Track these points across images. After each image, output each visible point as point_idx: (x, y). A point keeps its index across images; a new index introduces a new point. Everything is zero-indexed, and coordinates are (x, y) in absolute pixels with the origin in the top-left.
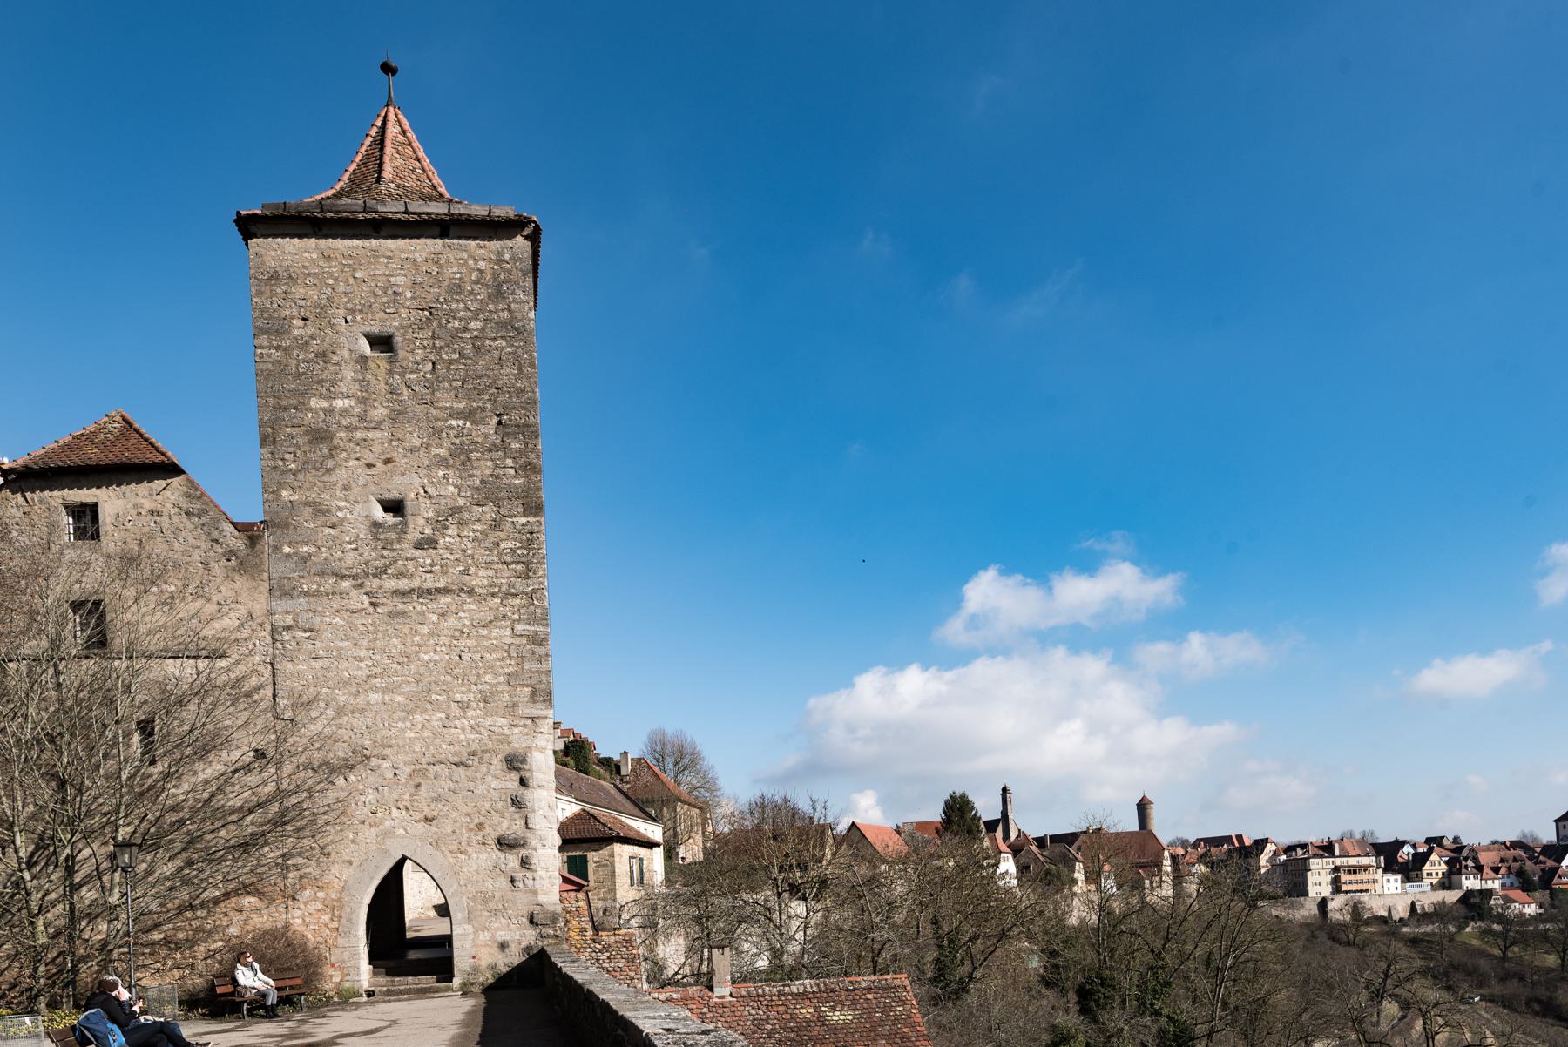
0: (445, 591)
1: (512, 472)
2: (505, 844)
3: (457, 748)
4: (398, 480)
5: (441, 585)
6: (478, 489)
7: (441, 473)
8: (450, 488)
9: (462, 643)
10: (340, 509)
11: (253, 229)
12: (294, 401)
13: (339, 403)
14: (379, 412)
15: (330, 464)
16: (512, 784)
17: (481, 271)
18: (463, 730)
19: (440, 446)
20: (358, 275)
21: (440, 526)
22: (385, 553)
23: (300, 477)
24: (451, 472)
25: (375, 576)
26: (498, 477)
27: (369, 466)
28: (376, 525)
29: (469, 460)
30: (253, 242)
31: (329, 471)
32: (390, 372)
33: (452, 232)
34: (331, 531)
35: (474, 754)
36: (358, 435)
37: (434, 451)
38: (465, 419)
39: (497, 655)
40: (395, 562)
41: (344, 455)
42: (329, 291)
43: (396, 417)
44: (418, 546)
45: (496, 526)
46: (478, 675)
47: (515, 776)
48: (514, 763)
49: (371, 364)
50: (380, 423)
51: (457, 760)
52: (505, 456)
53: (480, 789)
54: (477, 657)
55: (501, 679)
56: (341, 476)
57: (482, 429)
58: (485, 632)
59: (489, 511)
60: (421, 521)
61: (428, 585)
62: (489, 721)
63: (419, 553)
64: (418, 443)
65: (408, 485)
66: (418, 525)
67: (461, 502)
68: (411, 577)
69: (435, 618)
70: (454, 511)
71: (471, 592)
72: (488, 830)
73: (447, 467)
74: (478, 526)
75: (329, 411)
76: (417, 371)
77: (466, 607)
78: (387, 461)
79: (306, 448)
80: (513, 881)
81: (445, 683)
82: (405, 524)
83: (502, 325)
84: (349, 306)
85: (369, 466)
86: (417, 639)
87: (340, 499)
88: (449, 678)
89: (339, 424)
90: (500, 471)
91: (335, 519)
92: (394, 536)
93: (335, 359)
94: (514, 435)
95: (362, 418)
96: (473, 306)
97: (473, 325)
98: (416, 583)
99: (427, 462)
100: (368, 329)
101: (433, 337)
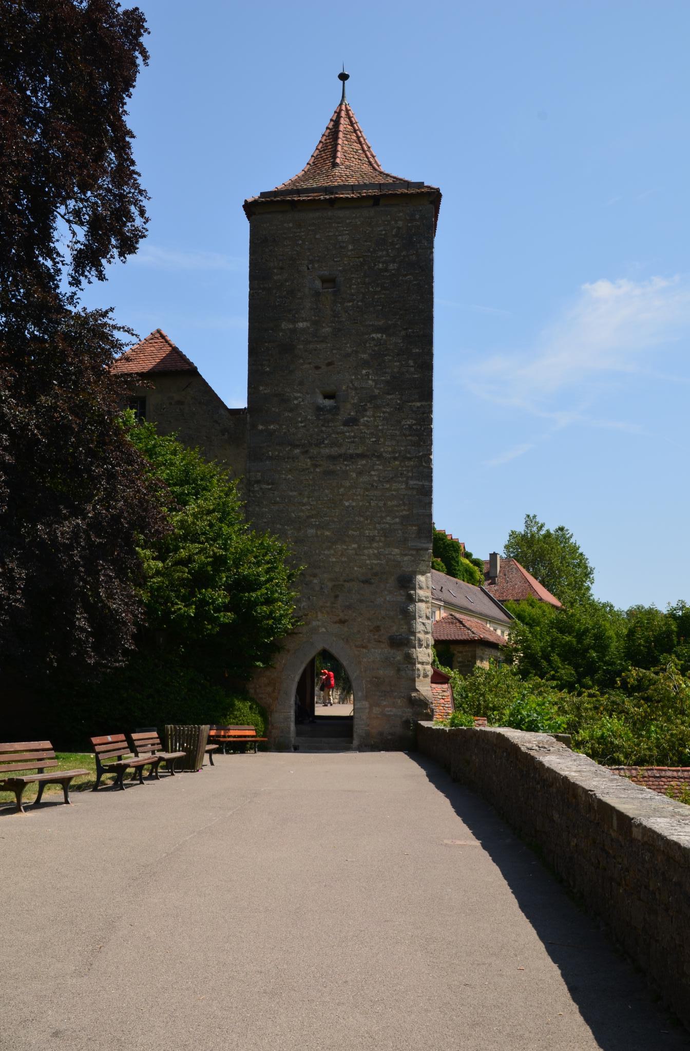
0: (362, 456)
1: (412, 369)
5: (359, 451)
7: (364, 372)
10: (296, 398)
13: (301, 325)
14: (327, 330)
16: (401, 598)
17: (399, 228)
20: (318, 236)
22: (324, 429)
28: (319, 409)
35: (376, 574)
36: (311, 346)
39: (395, 503)
42: (298, 249)
44: (346, 423)
46: (382, 517)
54: (381, 504)
58: (388, 486)
60: (349, 406)
63: (346, 429)
64: (349, 350)
66: (348, 410)
67: (377, 392)
69: (354, 475)
70: (373, 398)
71: (380, 457)
75: (294, 331)
76: (352, 300)
77: (376, 467)
78: (329, 364)
84: (311, 258)
85: (317, 368)
86: (342, 490)
88: (362, 519)
92: (329, 417)
93: (299, 295)
97: (391, 266)
98: (343, 451)
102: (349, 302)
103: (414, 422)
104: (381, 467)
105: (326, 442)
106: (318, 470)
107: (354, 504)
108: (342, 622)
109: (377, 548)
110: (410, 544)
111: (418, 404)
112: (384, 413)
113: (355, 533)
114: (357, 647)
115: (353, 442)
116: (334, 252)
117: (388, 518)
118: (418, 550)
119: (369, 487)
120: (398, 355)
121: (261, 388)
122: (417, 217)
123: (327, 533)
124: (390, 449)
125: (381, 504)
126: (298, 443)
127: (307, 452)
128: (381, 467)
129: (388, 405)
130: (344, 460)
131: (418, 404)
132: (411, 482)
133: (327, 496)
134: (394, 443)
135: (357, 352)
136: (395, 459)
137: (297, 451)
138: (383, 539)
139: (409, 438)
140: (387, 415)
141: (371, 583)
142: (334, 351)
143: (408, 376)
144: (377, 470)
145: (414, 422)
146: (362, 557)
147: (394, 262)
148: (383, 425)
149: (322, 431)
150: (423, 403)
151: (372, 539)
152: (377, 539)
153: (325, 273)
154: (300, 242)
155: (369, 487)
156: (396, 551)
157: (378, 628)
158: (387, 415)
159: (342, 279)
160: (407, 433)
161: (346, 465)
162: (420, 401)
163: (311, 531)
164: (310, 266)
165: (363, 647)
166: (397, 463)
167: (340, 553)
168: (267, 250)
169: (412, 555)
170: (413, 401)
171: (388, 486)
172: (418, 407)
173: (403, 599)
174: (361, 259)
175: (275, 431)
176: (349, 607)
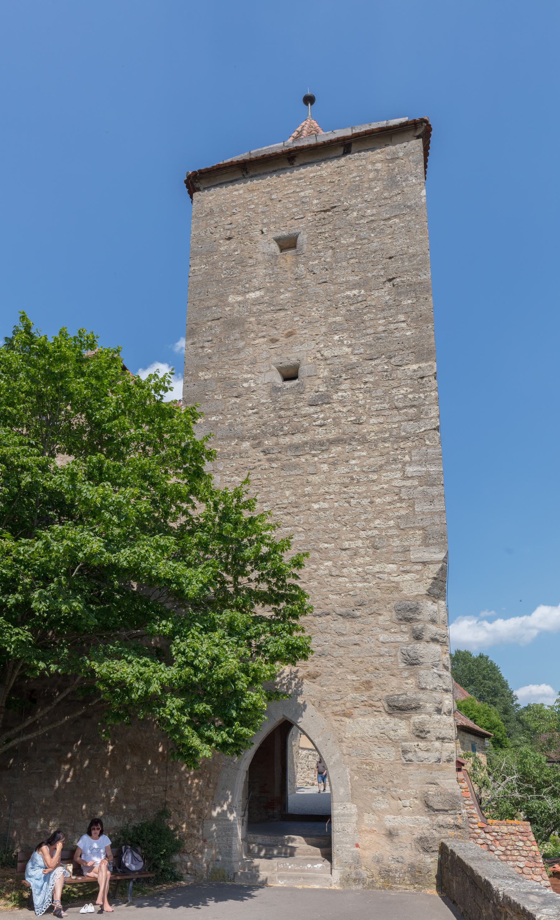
0: (337, 441)
2: (399, 708)
4: (296, 349)
5: (331, 436)
7: (336, 337)
8: (343, 349)
9: (352, 489)
10: (246, 380)
11: (197, 185)
17: (377, 171)
20: (273, 197)
21: (334, 383)
22: (282, 413)
24: (345, 335)
27: (274, 341)
30: (196, 195)
31: (239, 351)
33: (353, 149)
34: (238, 400)
36: (267, 317)
37: (331, 320)
38: (360, 288)
41: (252, 335)
47: (404, 628)
51: (343, 610)
52: (397, 314)
54: (365, 502)
58: (375, 477)
59: (381, 364)
63: (312, 409)
67: (354, 359)
68: (306, 431)
73: (343, 331)
77: (357, 454)
81: (333, 531)
84: (265, 221)
85: (274, 341)
86: (308, 489)
87: (248, 372)
90: (392, 326)
92: (291, 397)
100: (279, 234)
103: (410, 390)
105: (286, 428)
106: (274, 465)
107: (326, 505)
110: (413, 556)
111: (415, 367)
112: (366, 383)
114: (335, 714)
116: (294, 210)
117: (377, 522)
118: (424, 563)
119: (347, 481)
120: (383, 310)
122: (401, 154)
124: (376, 428)
125: (365, 502)
129: (371, 373)
131: (415, 367)
132: (410, 470)
133: (287, 498)
134: (381, 419)
135: (326, 317)
136: (384, 440)
137: (246, 445)
138: (371, 551)
142: (296, 319)
144: (359, 458)
145: (410, 390)
146: (341, 579)
149: (280, 417)
150: (421, 365)
152: (362, 551)
154: (253, 206)
155: (347, 481)
157: (368, 685)
159: (306, 236)
162: (417, 363)
164: (264, 230)
165: (345, 715)
166: (387, 445)
168: (212, 222)
169: (417, 572)
171: (375, 477)
173: (406, 638)
175: (217, 423)
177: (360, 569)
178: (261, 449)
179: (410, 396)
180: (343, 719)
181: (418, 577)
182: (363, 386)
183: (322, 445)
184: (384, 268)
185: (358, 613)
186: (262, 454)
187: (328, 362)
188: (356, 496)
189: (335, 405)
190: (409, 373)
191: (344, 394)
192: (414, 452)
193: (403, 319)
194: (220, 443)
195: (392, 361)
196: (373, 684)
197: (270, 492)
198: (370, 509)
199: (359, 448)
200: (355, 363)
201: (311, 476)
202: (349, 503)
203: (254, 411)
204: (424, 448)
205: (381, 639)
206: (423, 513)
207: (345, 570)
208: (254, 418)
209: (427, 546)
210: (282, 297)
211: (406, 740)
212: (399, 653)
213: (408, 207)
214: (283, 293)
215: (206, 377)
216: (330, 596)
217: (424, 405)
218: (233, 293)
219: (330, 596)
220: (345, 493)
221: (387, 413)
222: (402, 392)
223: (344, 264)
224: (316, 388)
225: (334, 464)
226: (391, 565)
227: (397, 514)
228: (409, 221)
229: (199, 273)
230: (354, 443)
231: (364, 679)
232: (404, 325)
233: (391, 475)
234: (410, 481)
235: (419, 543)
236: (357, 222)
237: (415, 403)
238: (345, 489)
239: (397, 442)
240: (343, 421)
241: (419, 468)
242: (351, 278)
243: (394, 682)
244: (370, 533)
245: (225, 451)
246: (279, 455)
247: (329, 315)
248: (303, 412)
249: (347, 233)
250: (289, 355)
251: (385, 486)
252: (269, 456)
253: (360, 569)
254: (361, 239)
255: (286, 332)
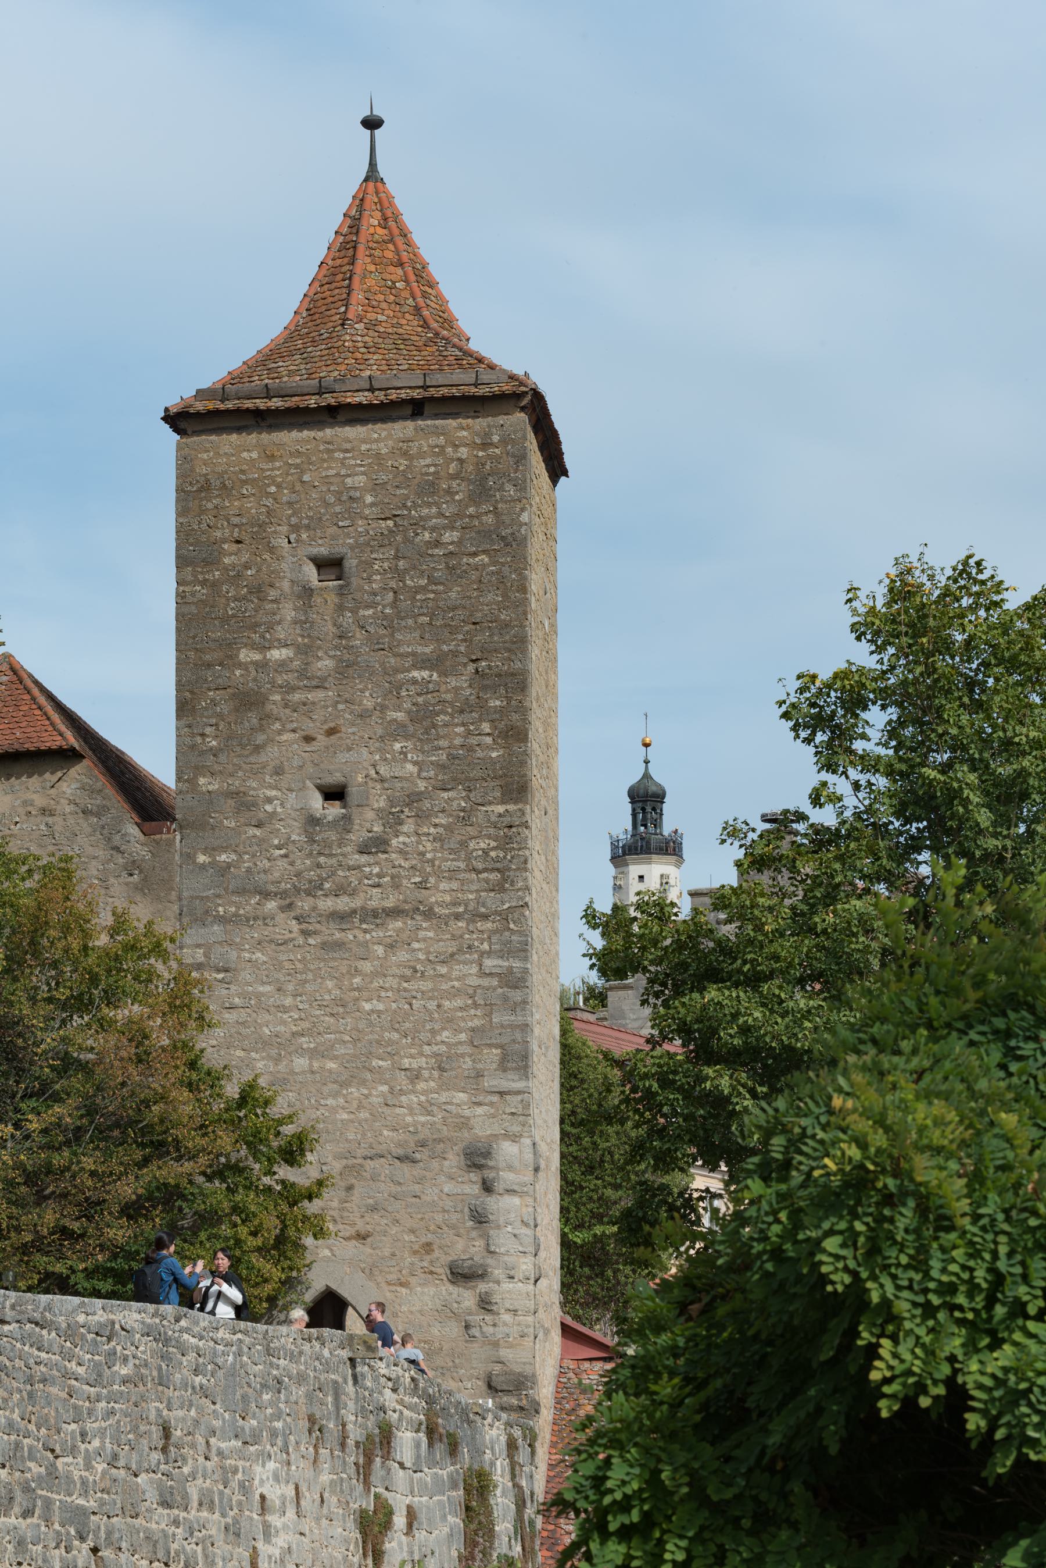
2: (462, 1275)
3: (402, 1137)
5: (389, 904)
6: (441, 767)
7: (397, 746)
10: (269, 800)
12: (218, 655)
13: (276, 654)
14: (325, 664)
15: (260, 738)
18: (411, 1109)
19: (399, 708)
22: (322, 860)
23: (222, 758)
25: (309, 893)
26: (471, 749)
27: (308, 739)
28: (313, 821)
29: (434, 726)
31: (258, 749)
32: (340, 608)
34: (258, 832)
36: (297, 697)
39: (459, 1002)
40: (334, 873)
41: (278, 726)
43: (345, 669)
44: (364, 850)
45: (465, 818)
46: (433, 1032)
47: (474, 1176)
48: (477, 1159)
49: (317, 600)
50: (323, 679)
51: (400, 1152)
52: (481, 720)
53: (430, 1194)
54: (432, 1005)
55: (463, 1037)
56: (271, 754)
57: (453, 682)
59: (456, 798)
60: (370, 815)
61: (373, 904)
62: (444, 1097)
63: (364, 859)
64: (369, 704)
65: (355, 762)
66: (368, 822)
67: (422, 785)
68: (353, 894)
69: (380, 950)
70: (414, 798)
71: (429, 914)
72: (437, 1253)
74: (442, 820)
75: (262, 666)
77: (422, 934)
78: (331, 732)
79: (232, 718)
80: (467, 1327)
81: (390, 1042)
82: (347, 818)
83: (485, 534)
85: (308, 739)
86: (357, 980)
87: (271, 787)
88: (396, 1036)
89: (273, 682)
90: (473, 741)
91: (261, 815)
92: (333, 836)
93: (273, 594)
94: (494, 688)
95: (302, 674)
96: (448, 510)
97: (448, 536)
98: (357, 903)
99: (380, 732)
101: (397, 557)
102: (368, 607)
103: (493, 844)
104: (431, 934)
105: (327, 886)
107: (381, 1007)
108: (361, 1237)
109: (425, 1092)
111: (500, 809)
112: (436, 826)
113: (381, 1063)
114: (389, 1283)
115: (378, 886)
117: (445, 1034)
118: (501, 1094)
119: (408, 972)
120: (462, 712)
121: (202, 781)
123: (331, 1065)
126: (272, 888)
127: (290, 906)
128: (431, 934)
129: (443, 811)
130: (362, 921)
131: (500, 809)
132: (489, 963)
134: (455, 885)
135: (383, 708)
136: (458, 917)
137: (272, 905)
138: (436, 1074)
139: (485, 875)
140: (441, 830)
141: (414, 1161)
143: (480, 754)
144: (424, 940)
145: (493, 844)
146: (398, 1110)
147: (453, 528)
148: (434, 850)
149: (319, 866)
150: (511, 807)
151: (415, 1076)
152: (426, 1074)
153: (322, 550)
155: (408, 972)
156: (462, 1096)
157: (428, 1247)
158: (441, 830)
159: (355, 562)
160: (480, 866)
161: (365, 931)
162: (503, 803)
163: (301, 1063)
165: (401, 1285)
166: (460, 924)
167: (355, 1104)
169: (491, 1104)
170: (490, 803)
172: (500, 816)
174: (390, 523)
176: (374, 1209)
177: (423, 1098)
178: (293, 914)
179: (493, 854)
180: (399, 1289)
181: (492, 1111)
182: (432, 830)
183: (376, 917)
184: (465, 640)
185: (418, 1156)
186: (294, 922)
187: (386, 785)
188: (419, 995)
189: (394, 856)
190: (493, 819)
191: (407, 840)
192: (494, 939)
193: (488, 730)
194: (235, 898)
195: (471, 795)
196: (435, 1247)
197: (306, 981)
198: (436, 1015)
199: (424, 925)
200: (422, 793)
201: (362, 962)
202: (411, 1005)
203: (282, 852)
204: (507, 933)
205: (446, 1190)
206: (502, 1026)
207: (403, 1098)
208: (282, 863)
209: (505, 1071)
210: (320, 664)
211: (470, 1314)
212: (466, 1210)
213: (503, 538)
214: (320, 659)
215: (210, 788)
216: (385, 1133)
217: (509, 869)
218: (246, 646)
219: (385, 1133)
220: (405, 990)
221: (462, 876)
222: (482, 845)
223: (410, 622)
224: (368, 825)
225: (391, 946)
226: (461, 1095)
227: (470, 1024)
228: (503, 564)
229: (190, 599)
230: (418, 918)
231: (424, 1240)
232: (489, 740)
233: (465, 969)
234: (489, 979)
235: (495, 1066)
236: (430, 552)
237: (498, 865)
238: (405, 985)
239: (474, 921)
240: (405, 882)
241: (500, 962)
242: (420, 649)
243: (460, 1244)
244: (435, 1048)
245: (242, 912)
246: (318, 926)
247: (387, 707)
248: (351, 863)
249: (414, 568)
250: (331, 767)
251: (456, 984)
252: (304, 926)
253: (423, 1098)
254: (436, 584)
255: (326, 727)
